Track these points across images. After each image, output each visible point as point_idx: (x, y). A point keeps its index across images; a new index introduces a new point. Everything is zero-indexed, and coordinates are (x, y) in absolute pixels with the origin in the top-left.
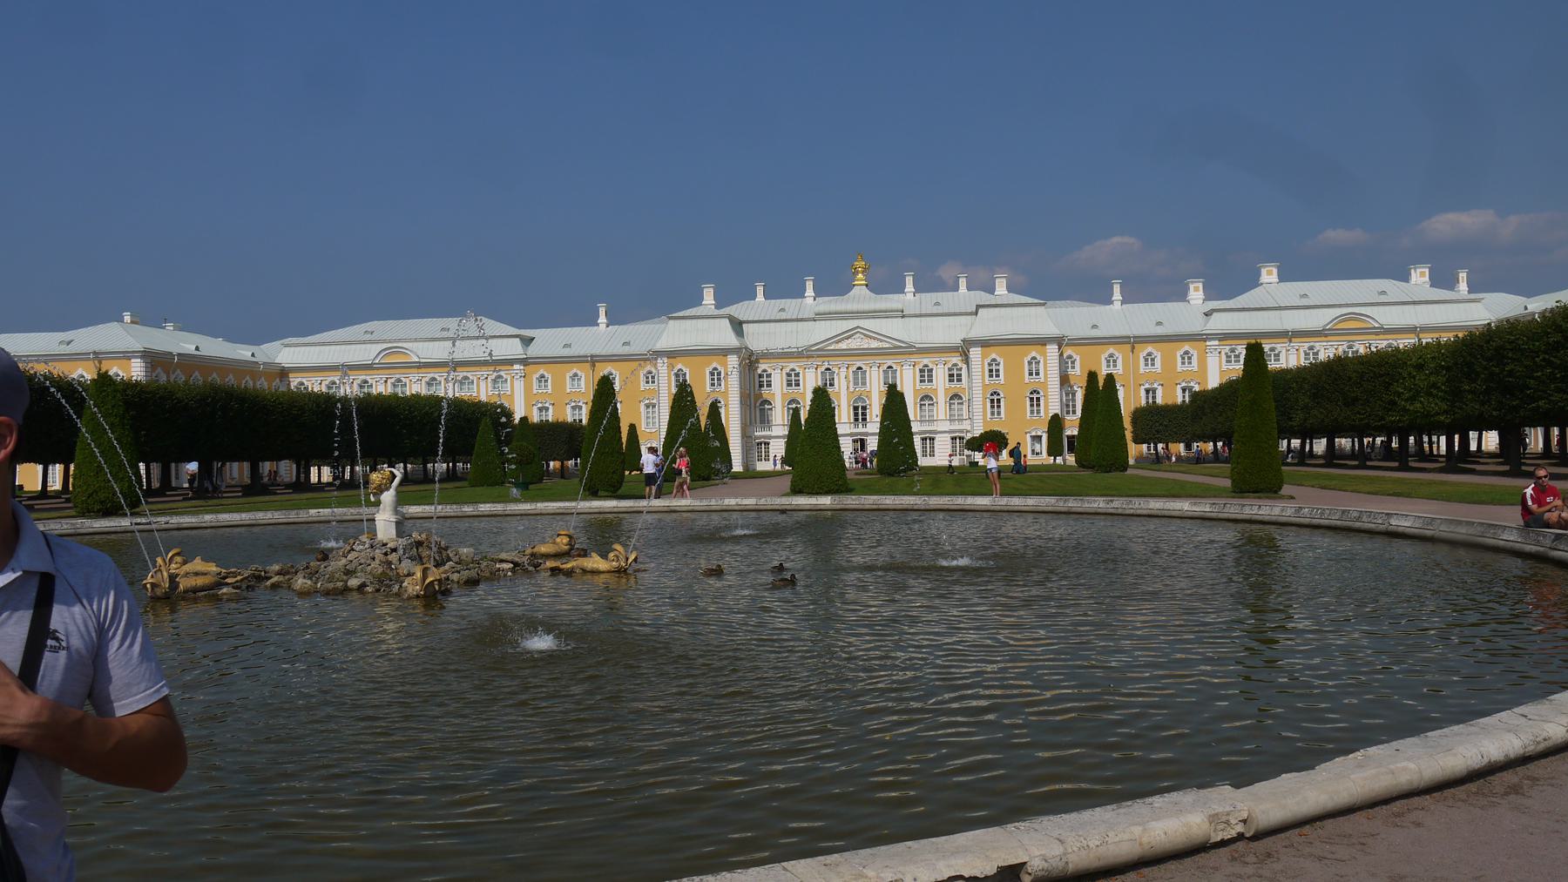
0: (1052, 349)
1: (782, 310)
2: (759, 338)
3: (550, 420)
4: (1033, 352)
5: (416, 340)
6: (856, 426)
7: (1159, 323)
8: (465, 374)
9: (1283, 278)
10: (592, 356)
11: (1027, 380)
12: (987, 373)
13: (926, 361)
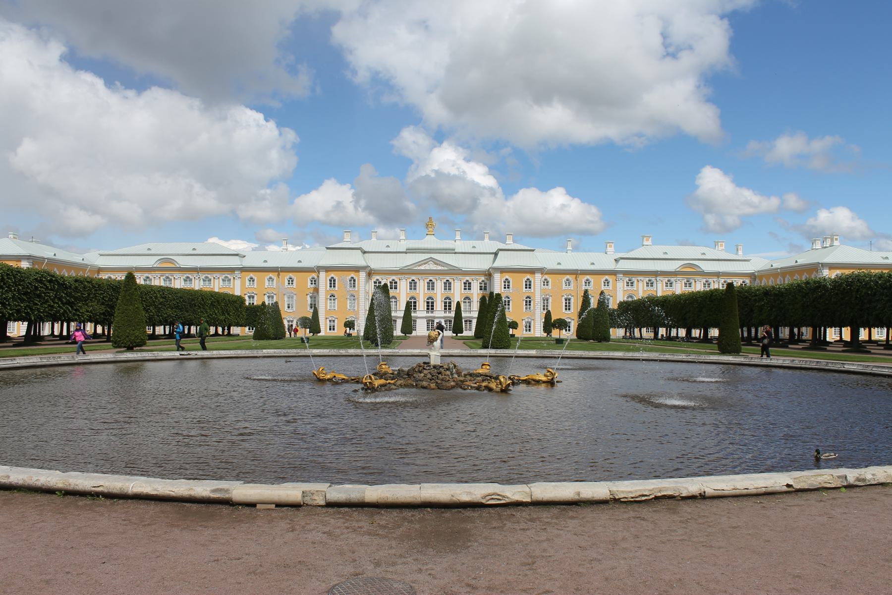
0: (538, 276)
1: (388, 246)
3: (255, 304)
4: (528, 276)
5: (178, 255)
6: (428, 312)
7: (593, 264)
8: (207, 275)
10: (281, 268)
11: (524, 291)
12: (503, 286)
13: (468, 278)
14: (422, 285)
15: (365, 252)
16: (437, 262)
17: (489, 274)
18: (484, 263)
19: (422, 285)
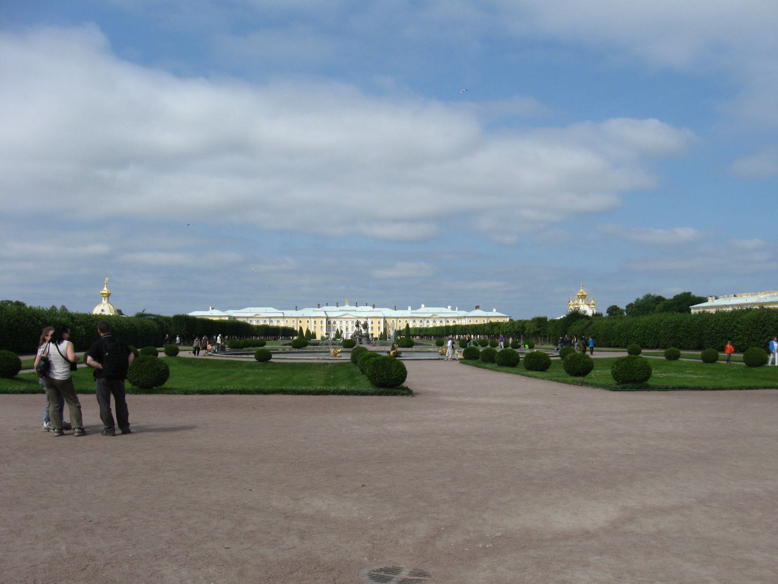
2: (330, 315)
4: (379, 320)
9: (425, 307)
14: (344, 323)
17: (367, 318)
18: (365, 315)
19: (344, 323)
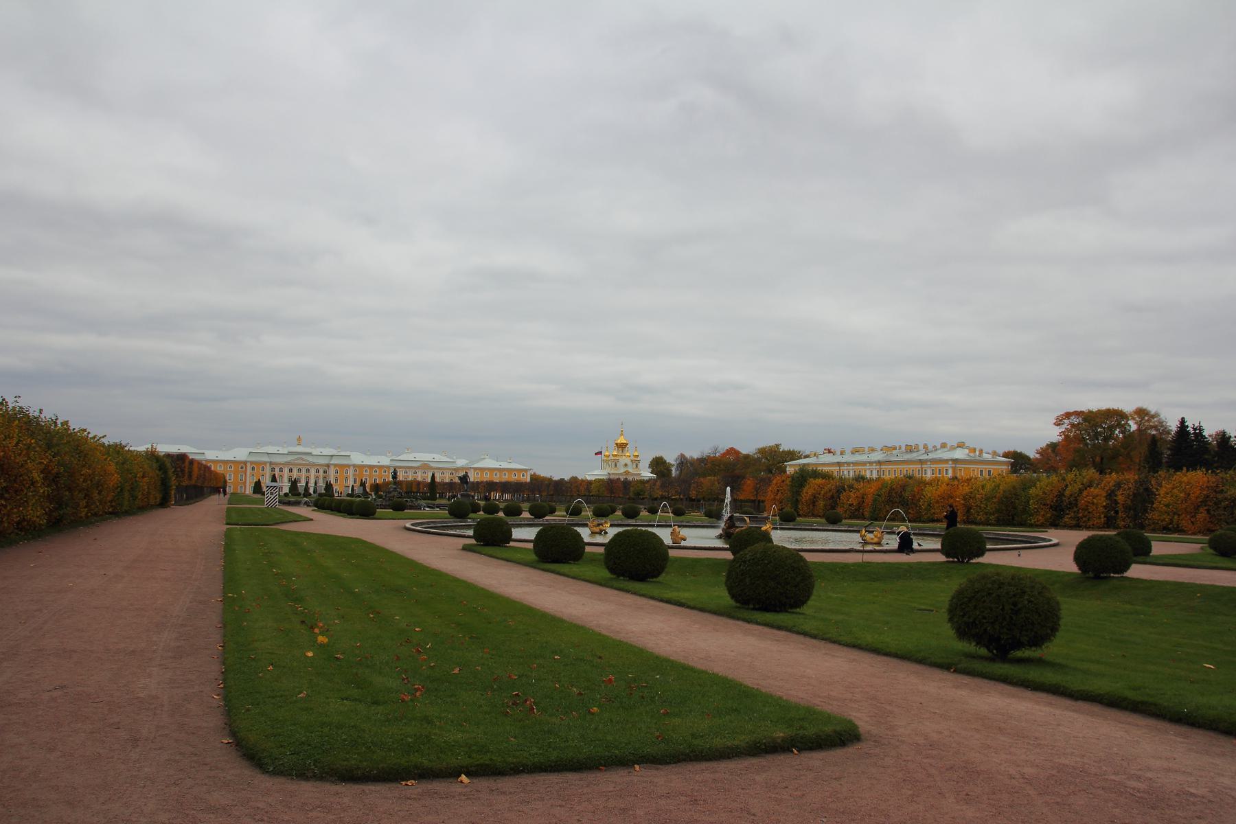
15: (268, 454)
16: (302, 459)
17: (328, 466)
